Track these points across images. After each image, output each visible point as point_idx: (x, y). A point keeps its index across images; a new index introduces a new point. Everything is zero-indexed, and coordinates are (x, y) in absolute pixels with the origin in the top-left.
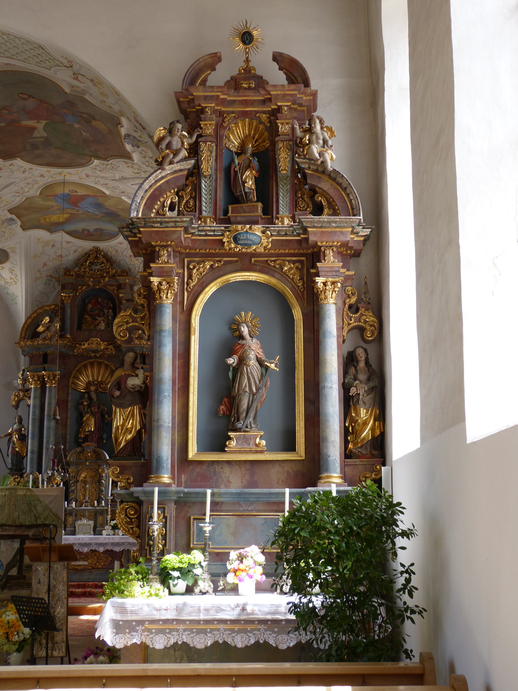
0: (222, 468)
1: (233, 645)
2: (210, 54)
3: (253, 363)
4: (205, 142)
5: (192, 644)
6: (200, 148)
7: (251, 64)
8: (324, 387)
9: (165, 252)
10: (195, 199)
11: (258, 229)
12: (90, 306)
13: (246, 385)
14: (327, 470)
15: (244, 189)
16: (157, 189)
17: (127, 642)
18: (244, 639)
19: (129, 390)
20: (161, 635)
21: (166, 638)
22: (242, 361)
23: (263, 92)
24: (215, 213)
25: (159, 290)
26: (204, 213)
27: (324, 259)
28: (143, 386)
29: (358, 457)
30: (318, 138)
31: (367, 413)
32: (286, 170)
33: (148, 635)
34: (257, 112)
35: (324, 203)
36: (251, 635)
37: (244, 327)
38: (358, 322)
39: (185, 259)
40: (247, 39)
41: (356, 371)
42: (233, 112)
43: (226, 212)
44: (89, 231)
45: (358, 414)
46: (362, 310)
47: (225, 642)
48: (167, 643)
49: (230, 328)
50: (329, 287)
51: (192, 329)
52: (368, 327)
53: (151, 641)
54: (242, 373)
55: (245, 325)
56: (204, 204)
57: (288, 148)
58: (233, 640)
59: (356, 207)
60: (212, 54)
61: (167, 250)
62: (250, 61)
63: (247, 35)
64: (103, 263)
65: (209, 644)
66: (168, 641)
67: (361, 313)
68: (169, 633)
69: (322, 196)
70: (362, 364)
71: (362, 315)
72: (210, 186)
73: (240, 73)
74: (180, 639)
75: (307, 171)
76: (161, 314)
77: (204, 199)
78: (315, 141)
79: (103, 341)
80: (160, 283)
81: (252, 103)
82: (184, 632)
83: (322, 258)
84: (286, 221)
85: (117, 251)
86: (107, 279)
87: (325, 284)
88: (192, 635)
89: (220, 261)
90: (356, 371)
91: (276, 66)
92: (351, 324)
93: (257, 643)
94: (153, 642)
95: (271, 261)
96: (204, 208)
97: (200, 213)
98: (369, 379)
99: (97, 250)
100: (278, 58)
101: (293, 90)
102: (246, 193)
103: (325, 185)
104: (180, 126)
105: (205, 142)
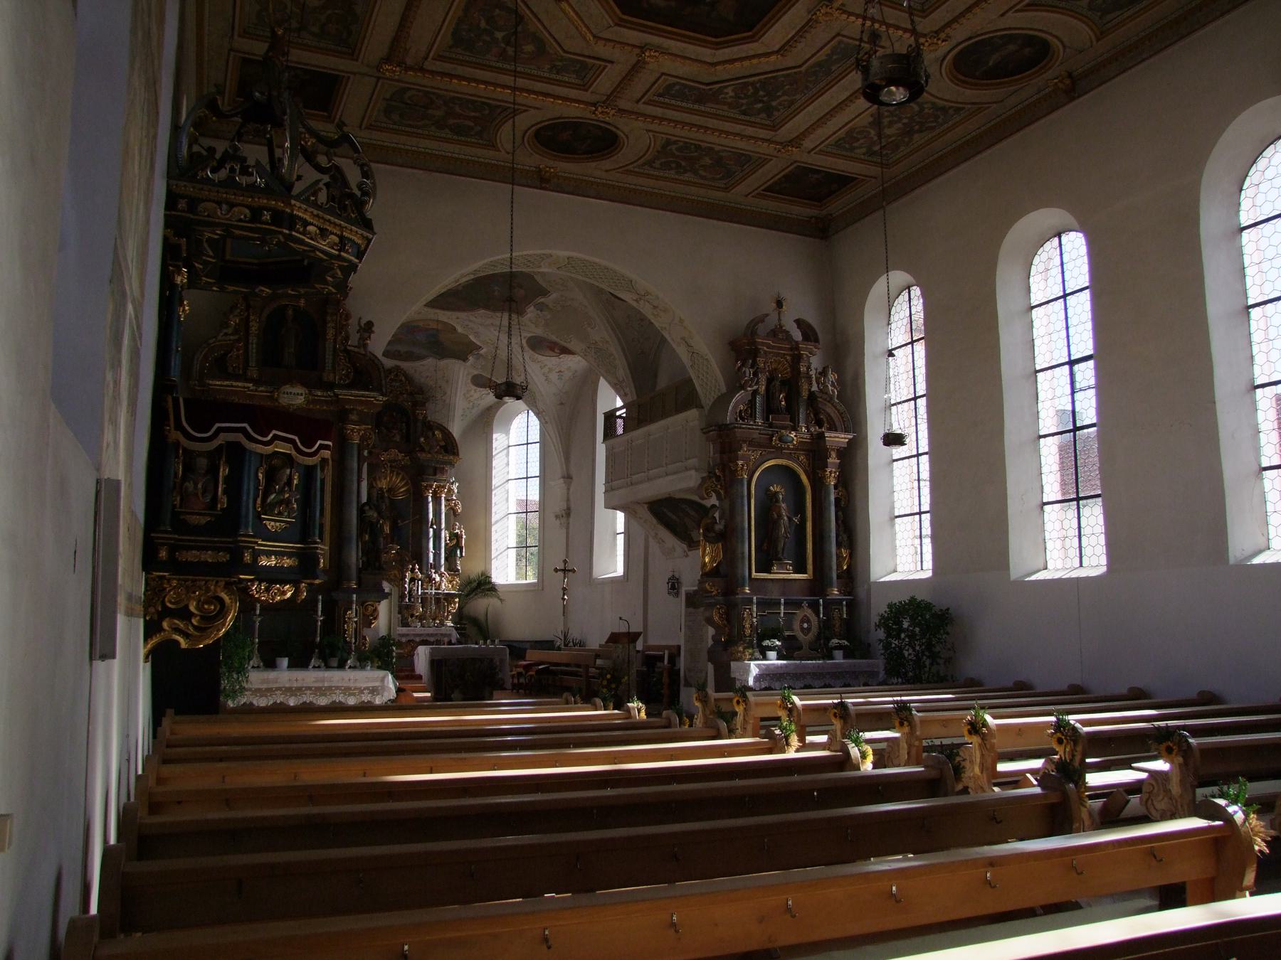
3: (785, 518)
10: (751, 408)
11: (793, 434)
12: (385, 418)
14: (831, 585)
22: (780, 516)
25: (742, 469)
30: (829, 380)
34: (784, 354)
35: (825, 420)
44: (399, 352)
64: (401, 381)
79: (401, 453)
84: (804, 429)
85: (416, 371)
86: (405, 396)
99: (397, 367)
100: (799, 322)
103: (830, 410)
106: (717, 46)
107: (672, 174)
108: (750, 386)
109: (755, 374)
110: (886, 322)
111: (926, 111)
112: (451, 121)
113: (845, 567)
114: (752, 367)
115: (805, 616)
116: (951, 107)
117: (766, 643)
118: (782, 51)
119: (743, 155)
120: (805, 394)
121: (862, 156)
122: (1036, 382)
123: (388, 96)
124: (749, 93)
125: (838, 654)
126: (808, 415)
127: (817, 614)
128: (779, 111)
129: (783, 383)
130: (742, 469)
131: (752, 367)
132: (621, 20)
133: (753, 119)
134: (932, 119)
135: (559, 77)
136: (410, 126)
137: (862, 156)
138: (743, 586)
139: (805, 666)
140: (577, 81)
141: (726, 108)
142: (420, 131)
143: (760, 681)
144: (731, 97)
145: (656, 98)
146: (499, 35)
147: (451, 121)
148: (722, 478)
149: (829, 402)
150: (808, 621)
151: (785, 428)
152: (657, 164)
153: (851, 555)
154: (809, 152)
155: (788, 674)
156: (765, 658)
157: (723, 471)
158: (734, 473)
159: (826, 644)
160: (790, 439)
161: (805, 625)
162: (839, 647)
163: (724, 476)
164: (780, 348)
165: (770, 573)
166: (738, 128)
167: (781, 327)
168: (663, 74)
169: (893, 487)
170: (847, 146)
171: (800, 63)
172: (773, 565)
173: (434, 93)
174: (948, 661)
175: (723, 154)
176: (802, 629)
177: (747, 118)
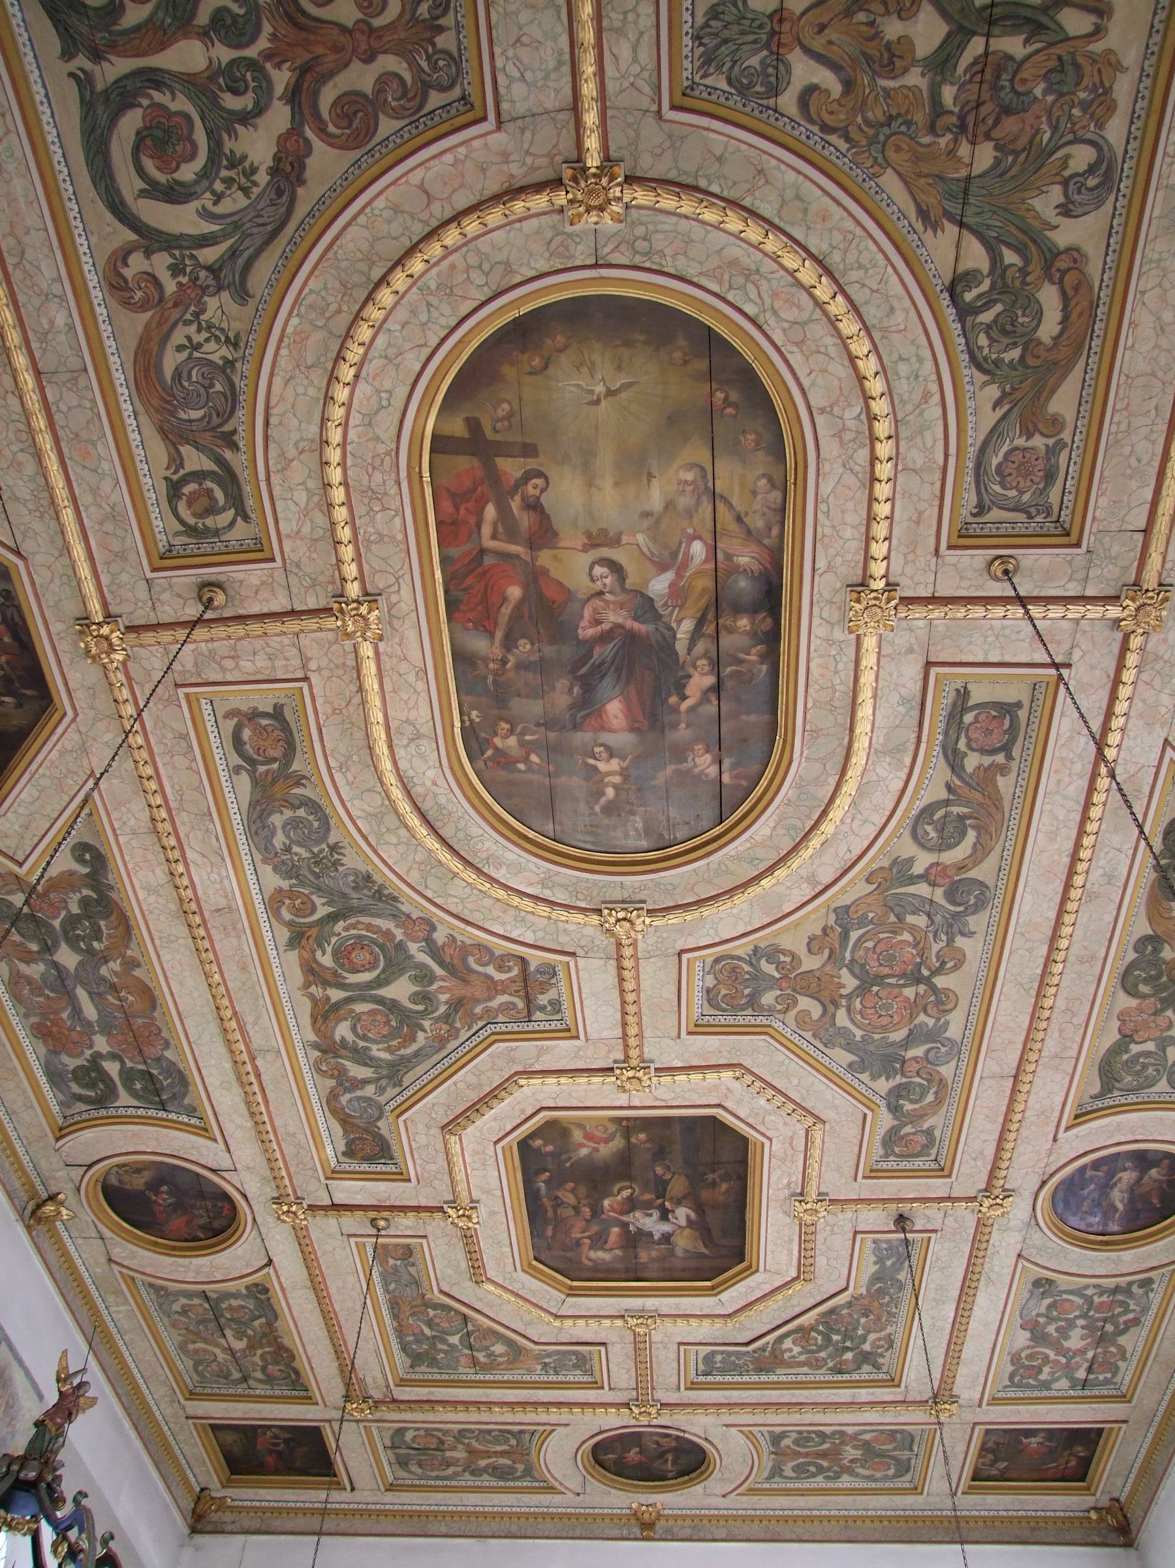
106: (714, 1291)
107: (819, 1482)
111: (1096, 1299)
112: (483, 1463)
116: (1130, 1284)
118: (804, 1271)
119: (896, 1431)
121: (1072, 1393)
123: (388, 1443)
124: (820, 1342)
128: (882, 1356)
132: (571, 1288)
133: (855, 1377)
134: (1118, 1310)
135: (560, 1378)
136: (437, 1478)
137: (1072, 1393)
140: (586, 1379)
141: (805, 1369)
142: (454, 1483)
144: (800, 1353)
145: (702, 1379)
146: (455, 1340)
147: (483, 1463)
152: (788, 1470)
154: (980, 1406)
166: (844, 1395)
168: (680, 1344)
170: (1031, 1381)
171: (844, 1285)
173: (439, 1430)
175: (867, 1437)
177: (846, 1377)
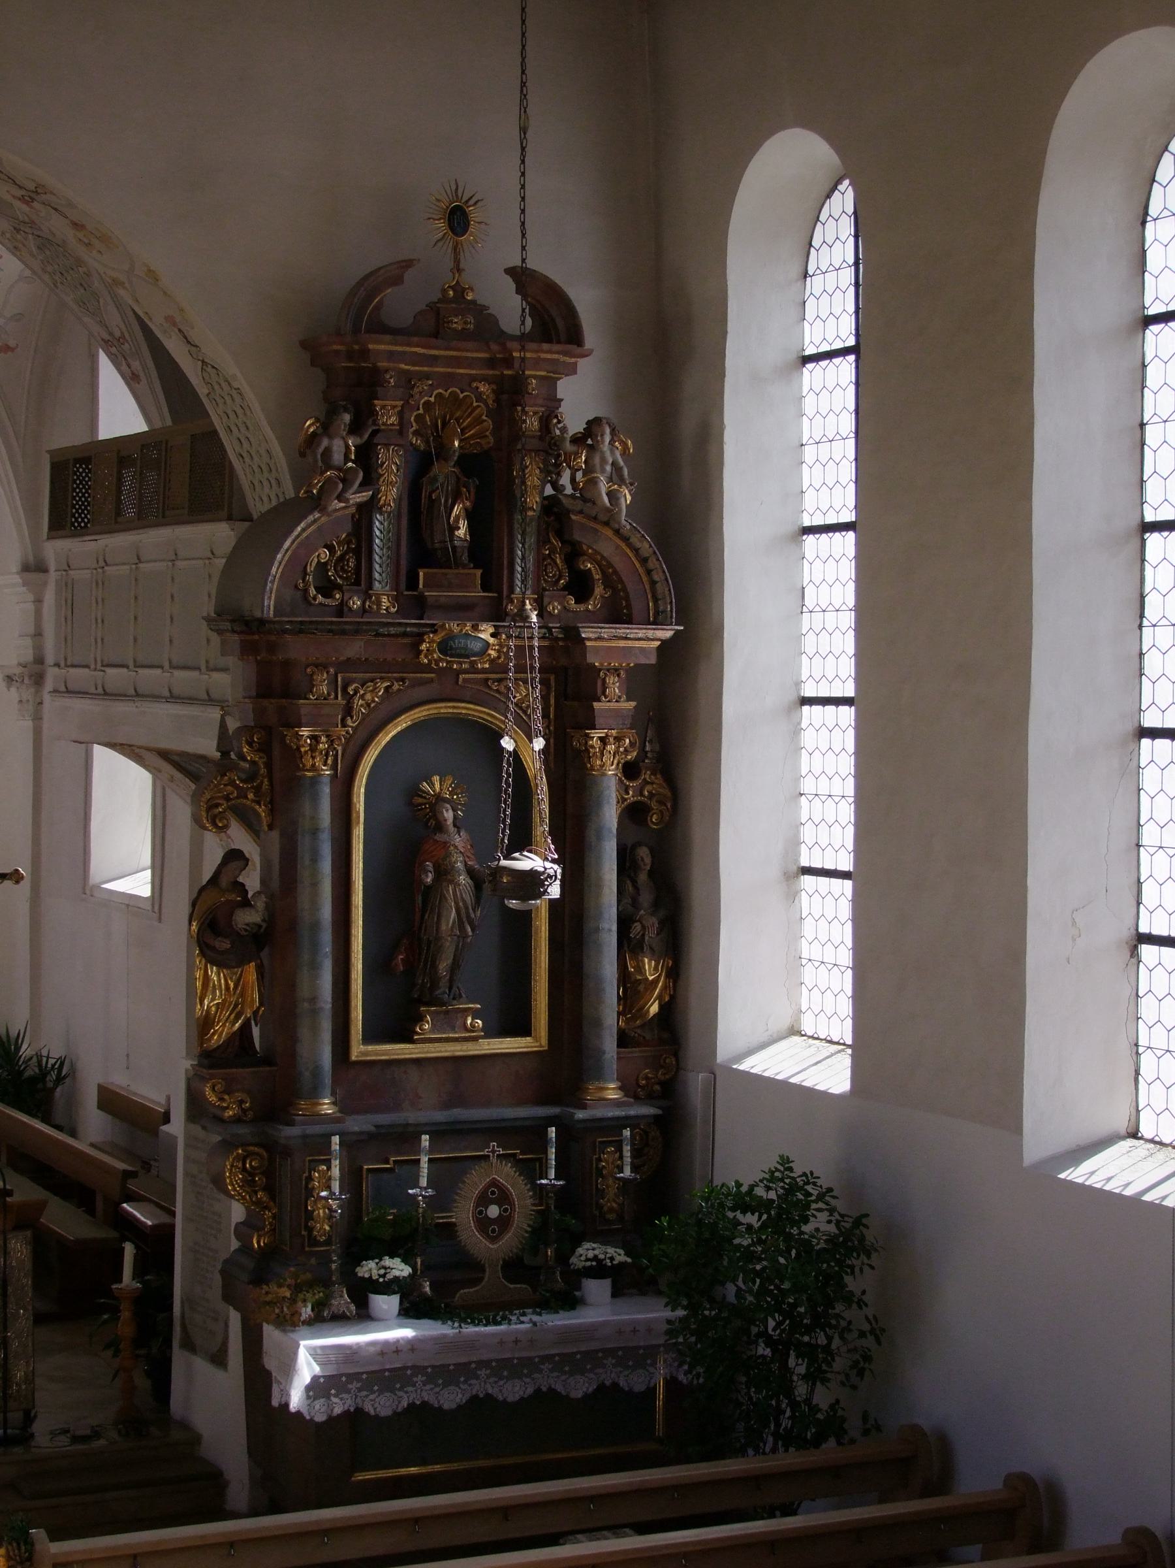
0: (405, 1072)
1: (501, 1399)
2: (398, 262)
3: (463, 879)
4: (387, 446)
5: (436, 1402)
6: (378, 458)
7: (466, 279)
8: (597, 930)
9: (325, 675)
10: (357, 552)
11: (486, 633)
13: (454, 922)
14: (599, 1074)
15: (452, 540)
16: (300, 544)
17: (332, 1410)
18: (517, 1389)
19: (238, 933)
20: (388, 1394)
21: (396, 1398)
22: (444, 873)
23: (494, 347)
24: (396, 587)
25: (313, 749)
26: (377, 585)
27: (604, 693)
28: (264, 925)
29: (637, 1044)
30: (603, 460)
31: (656, 969)
32: (534, 510)
33: (367, 1396)
34: (473, 378)
36: (528, 1380)
37: (447, 810)
38: (637, 796)
39: (339, 675)
40: (459, 223)
41: (636, 887)
42: (427, 376)
43: (412, 583)
45: (640, 969)
46: (646, 775)
47: (488, 1395)
48: (397, 1406)
49: (410, 804)
50: (611, 748)
51: (354, 815)
52: (654, 805)
53: (373, 1405)
54: (443, 898)
55: (448, 806)
56: (377, 567)
57: (539, 468)
58: (501, 1391)
59: (664, 598)
60: (402, 261)
61: (327, 673)
62: (464, 270)
63: (458, 214)
65: (464, 1401)
66: (399, 1402)
67: (645, 779)
68: (401, 1389)
69: (592, 559)
70: (643, 877)
71: (646, 782)
72: (389, 532)
73: (444, 299)
74: (418, 1397)
75: (573, 517)
76: (315, 799)
77: (377, 558)
78: (598, 467)
80: (315, 739)
81: (470, 363)
82: (424, 1385)
83: (599, 691)
87: (603, 740)
88: (437, 1389)
89: (403, 680)
90: (636, 887)
91: (510, 284)
92: (626, 800)
93: (538, 1391)
94: (375, 1406)
95: (495, 680)
96: (377, 576)
97: (370, 586)
98: (656, 905)
100: (522, 277)
101: (550, 353)
102: (454, 548)
103: (607, 546)
104: (347, 418)
105: (387, 446)
108: (340, 498)
109: (366, 457)
110: (795, 270)
113: (654, 1009)
114: (354, 429)
115: (494, 1183)
117: (369, 1269)
120: (533, 501)
122: (1143, 560)
125: (597, 1290)
126: (542, 563)
127: (531, 1169)
129: (470, 463)
130: (313, 749)
131: (354, 429)
138: (315, 1094)
139: (471, 1344)
143: (328, 1396)
148: (263, 771)
149: (607, 524)
150: (503, 1198)
151: (462, 609)
153: (675, 973)
155: (418, 1369)
156: (363, 1315)
157: (265, 748)
158: (293, 756)
159: (563, 1259)
160: (477, 646)
161: (493, 1211)
162: (598, 1270)
163: (269, 765)
164: (458, 362)
165: (412, 1041)
167: (460, 291)
169: (798, 778)
172: (420, 1019)
174: (861, 1365)
176: (483, 1223)
